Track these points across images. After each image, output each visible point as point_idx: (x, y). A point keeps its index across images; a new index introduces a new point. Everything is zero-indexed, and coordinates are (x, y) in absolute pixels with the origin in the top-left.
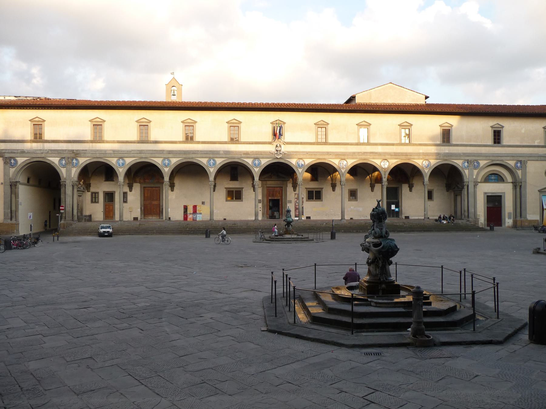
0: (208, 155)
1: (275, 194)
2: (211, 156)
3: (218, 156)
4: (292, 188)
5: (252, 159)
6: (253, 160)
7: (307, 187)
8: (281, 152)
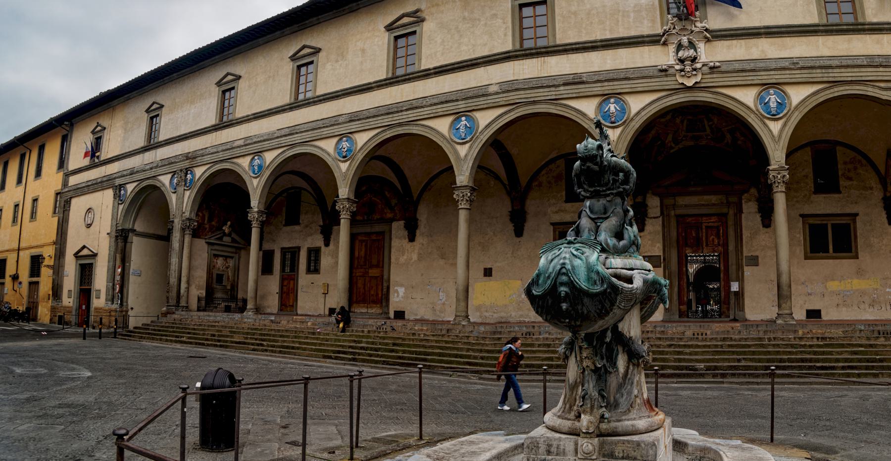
0: (450, 107)
1: (704, 239)
2: (462, 105)
3: (481, 102)
4: (758, 218)
5: (596, 102)
6: (600, 104)
8: (698, 66)
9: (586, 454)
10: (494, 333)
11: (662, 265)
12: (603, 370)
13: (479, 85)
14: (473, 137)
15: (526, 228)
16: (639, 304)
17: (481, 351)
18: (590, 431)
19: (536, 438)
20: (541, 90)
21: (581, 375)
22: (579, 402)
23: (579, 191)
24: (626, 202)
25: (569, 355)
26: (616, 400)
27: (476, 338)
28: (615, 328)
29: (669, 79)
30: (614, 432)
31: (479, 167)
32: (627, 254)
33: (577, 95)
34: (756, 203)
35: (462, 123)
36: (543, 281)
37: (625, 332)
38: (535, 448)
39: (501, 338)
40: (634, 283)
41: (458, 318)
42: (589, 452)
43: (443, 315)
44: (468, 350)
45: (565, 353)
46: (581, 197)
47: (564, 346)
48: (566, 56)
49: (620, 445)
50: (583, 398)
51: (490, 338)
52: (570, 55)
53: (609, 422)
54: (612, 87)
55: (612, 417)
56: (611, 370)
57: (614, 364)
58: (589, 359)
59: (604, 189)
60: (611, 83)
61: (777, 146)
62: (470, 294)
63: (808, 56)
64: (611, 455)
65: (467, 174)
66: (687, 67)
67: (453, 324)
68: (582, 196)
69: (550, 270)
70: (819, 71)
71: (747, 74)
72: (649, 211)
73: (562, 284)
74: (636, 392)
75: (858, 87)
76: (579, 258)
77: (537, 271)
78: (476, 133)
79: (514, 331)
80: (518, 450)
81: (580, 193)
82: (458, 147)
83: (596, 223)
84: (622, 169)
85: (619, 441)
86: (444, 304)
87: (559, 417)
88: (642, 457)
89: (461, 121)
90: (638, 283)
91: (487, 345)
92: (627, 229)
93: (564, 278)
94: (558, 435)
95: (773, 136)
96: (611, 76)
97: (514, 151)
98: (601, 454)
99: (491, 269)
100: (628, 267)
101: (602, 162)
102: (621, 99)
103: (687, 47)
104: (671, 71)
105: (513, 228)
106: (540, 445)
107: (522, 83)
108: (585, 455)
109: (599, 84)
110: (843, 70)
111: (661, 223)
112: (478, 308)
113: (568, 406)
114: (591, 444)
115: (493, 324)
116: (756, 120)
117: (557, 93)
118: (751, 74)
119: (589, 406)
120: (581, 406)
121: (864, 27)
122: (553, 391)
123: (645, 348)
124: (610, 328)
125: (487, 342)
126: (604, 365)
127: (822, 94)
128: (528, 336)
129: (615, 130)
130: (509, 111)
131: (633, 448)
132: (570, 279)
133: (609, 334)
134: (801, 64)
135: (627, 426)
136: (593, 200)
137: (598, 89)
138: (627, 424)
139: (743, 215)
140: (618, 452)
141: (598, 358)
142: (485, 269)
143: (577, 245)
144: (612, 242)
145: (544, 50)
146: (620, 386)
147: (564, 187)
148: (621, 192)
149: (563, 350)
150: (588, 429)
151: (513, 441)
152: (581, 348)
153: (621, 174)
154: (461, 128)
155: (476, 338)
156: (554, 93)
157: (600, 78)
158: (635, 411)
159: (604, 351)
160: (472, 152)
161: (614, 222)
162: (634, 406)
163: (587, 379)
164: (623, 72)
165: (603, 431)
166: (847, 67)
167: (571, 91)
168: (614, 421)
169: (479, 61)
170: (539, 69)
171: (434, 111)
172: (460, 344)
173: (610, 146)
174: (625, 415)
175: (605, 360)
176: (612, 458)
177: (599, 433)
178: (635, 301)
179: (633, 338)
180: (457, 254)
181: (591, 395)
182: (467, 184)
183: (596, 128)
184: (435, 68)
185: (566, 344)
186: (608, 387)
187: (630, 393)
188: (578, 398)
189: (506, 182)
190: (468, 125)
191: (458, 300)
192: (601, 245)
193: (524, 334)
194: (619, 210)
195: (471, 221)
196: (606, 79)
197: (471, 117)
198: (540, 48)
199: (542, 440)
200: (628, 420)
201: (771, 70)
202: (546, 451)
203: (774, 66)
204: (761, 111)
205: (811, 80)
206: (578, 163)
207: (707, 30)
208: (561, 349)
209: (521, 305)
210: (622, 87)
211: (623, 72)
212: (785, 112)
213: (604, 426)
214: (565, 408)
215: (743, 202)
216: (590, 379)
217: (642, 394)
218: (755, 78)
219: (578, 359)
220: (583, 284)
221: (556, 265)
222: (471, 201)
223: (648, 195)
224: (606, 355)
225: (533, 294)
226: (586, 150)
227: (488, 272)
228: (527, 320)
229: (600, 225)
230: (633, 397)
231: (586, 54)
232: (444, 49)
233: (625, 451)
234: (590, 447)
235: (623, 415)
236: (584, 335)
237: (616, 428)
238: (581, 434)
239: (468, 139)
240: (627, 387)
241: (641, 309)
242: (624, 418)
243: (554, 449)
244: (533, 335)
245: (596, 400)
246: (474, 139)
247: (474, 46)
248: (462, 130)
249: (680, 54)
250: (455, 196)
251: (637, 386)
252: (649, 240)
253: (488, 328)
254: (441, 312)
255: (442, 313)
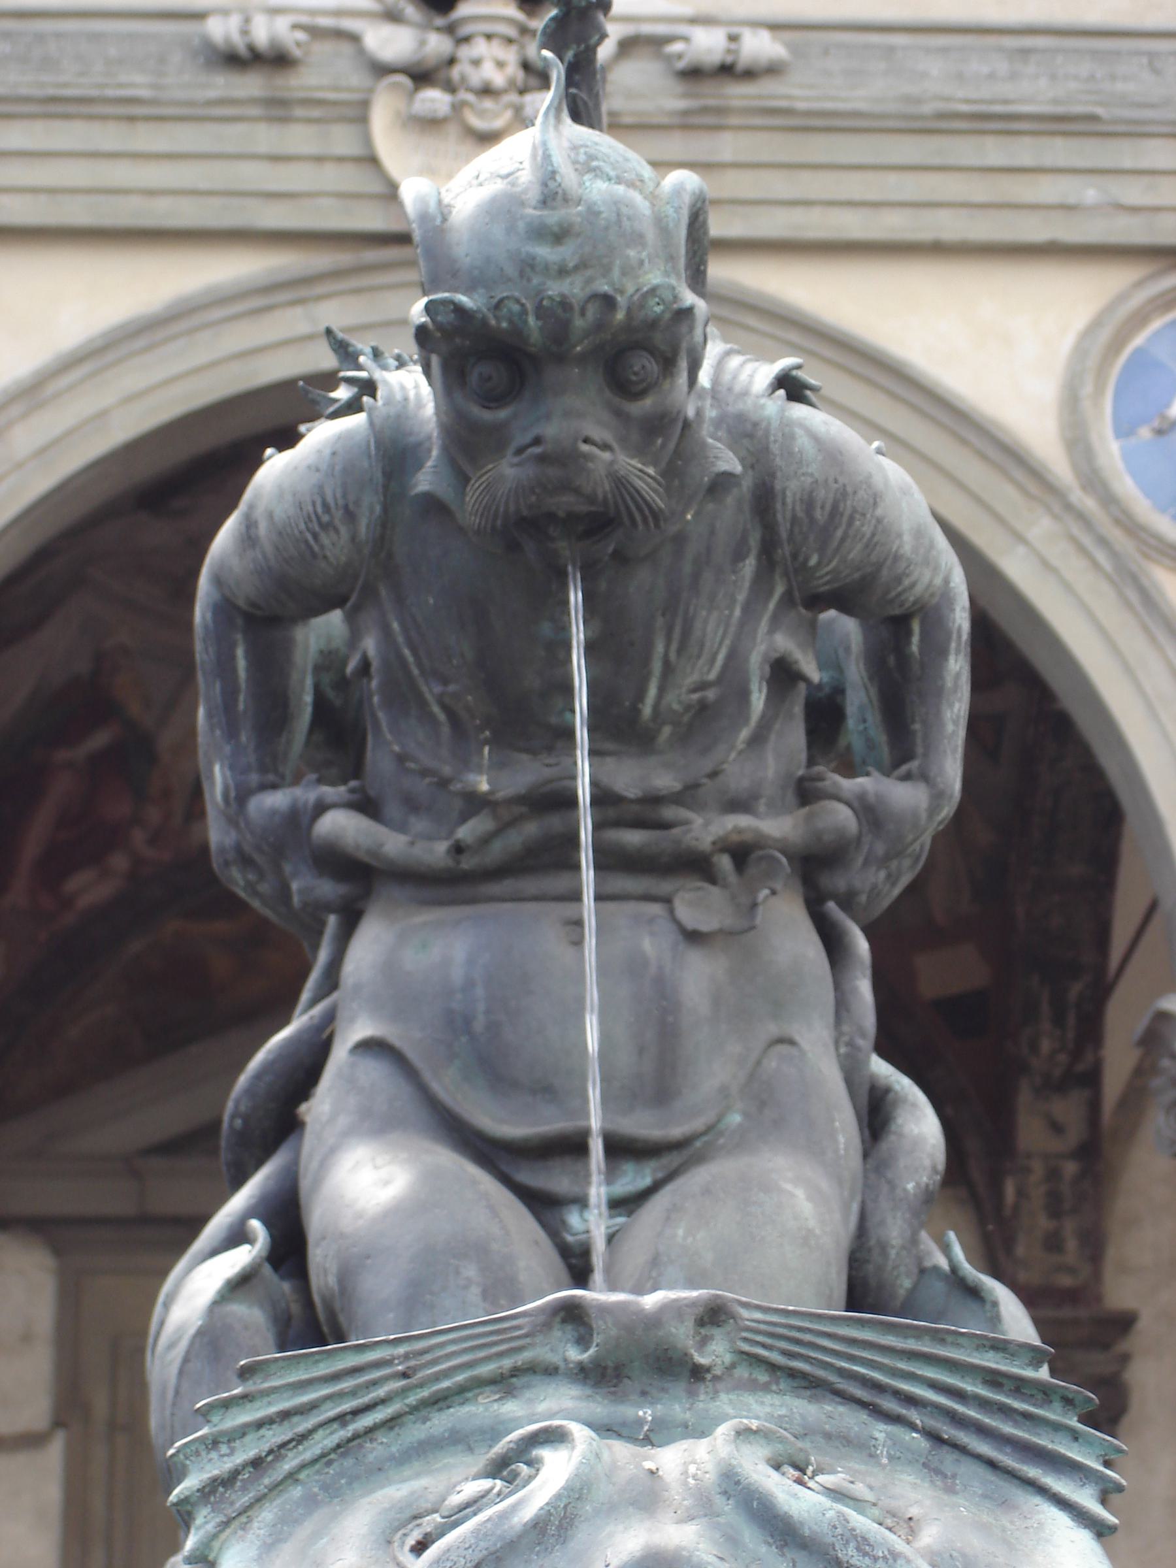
66: (480, 48)
71: (1024, 151)
116: (1074, 568)
118: (1059, 151)
204: (1127, 486)
218: (1090, 193)
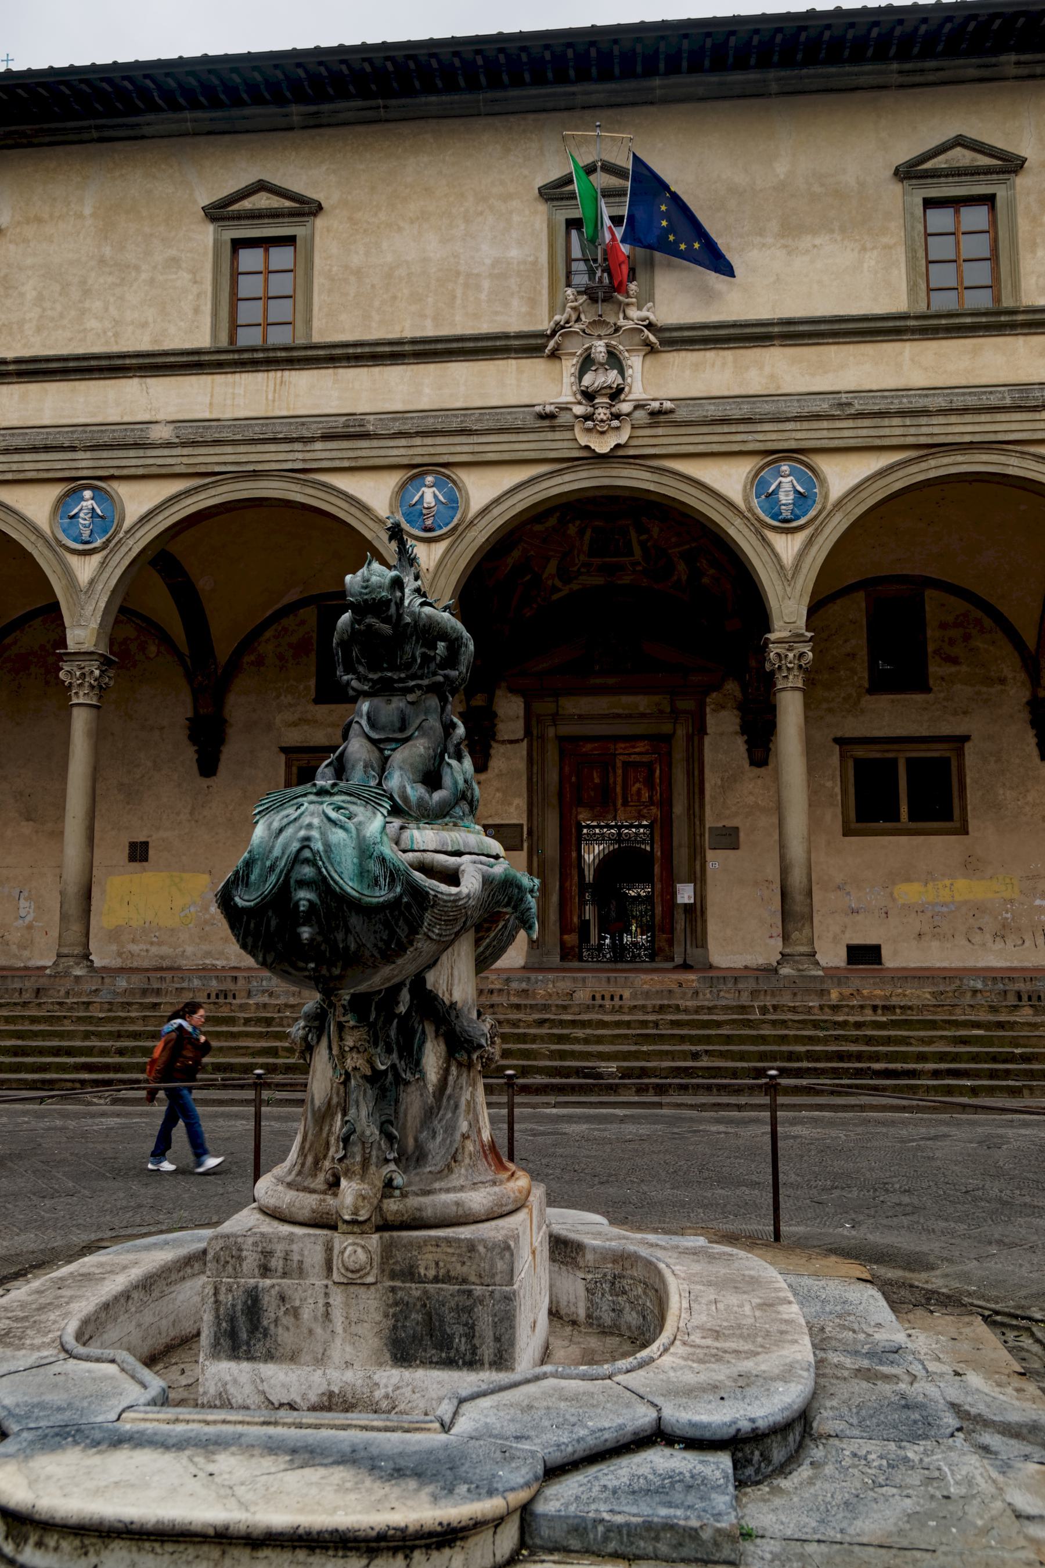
1: (619, 789)
2: (84, 463)
3: (131, 459)
4: (740, 745)
6: (403, 487)
7: (848, 734)
8: (625, 407)
9: (352, 1272)
10: (144, 992)
11: (525, 845)
12: (390, 1076)
13: (126, 419)
14: (109, 541)
15: (224, 757)
16: (471, 933)
17: (119, 1035)
18: (361, 1219)
19: (237, 1236)
20: (272, 447)
21: (342, 1088)
22: (336, 1151)
23: (345, 678)
24: (449, 707)
25: (314, 1043)
26: (419, 1146)
27: (106, 1006)
28: (418, 983)
29: (558, 435)
30: (414, 1219)
31: (122, 610)
32: (447, 819)
33: (353, 464)
34: (736, 712)
35: (84, 504)
36: (260, 876)
37: (442, 991)
38: (232, 1261)
39: (159, 1004)
40: (463, 881)
41: (63, 960)
42: (357, 1266)
43: (26, 953)
44: (87, 1035)
45: (305, 1038)
46: (351, 693)
47: (302, 1023)
48: (331, 371)
49: (430, 1248)
50: (346, 1140)
51: (141, 1004)
52: (341, 371)
53: (404, 1195)
54: (432, 450)
55: (410, 1184)
56: (408, 1076)
57: (416, 1064)
58: (359, 1052)
59: (403, 675)
60: (429, 441)
61: (789, 589)
62: (94, 902)
63: (875, 388)
64: (410, 1274)
65: (94, 624)
66: (600, 410)
67: (50, 976)
68: (354, 689)
69: (277, 852)
70: (896, 421)
72: (501, 726)
73: (302, 884)
74: (464, 1126)
75: (985, 458)
76: (342, 827)
77: (246, 854)
78: (116, 532)
79: (189, 989)
80: (192, 1267)
81: (348, 682)
82: (74, 561)
83: (381, 751)
84: (443, 634)
85: (426, 1241)
86: (30, 927)
87: (290, 1185)
88: (480, 1277)
89: (83, 499)
90: (470, 884)
91: (132, 1020)
92: (449, 764)
93: (307, 871)
94: (286, 1229)
95: (782, 567)
96: (430, 424)
97: (204, 584)
98: (387, 1273)
99: (145, 845)
100: (450, 849)
101: (400, 616)
102: (448, 477)
103: (602, 364)
104: (564, 418)
105: (196, 756)
106: (244, 1253)
107: (229, 427)
108: (350, 1275)
109: (403, 442)
110: (953, 419)
111: (525, 753)
112: (115, 935)
113: (310, 1160)
114: (363, 1247)
115: (147, 970)
116: (746, 531)
117: (308, 456)
118: (742, 428)
119: (358, 1158)
120: (341, 1160)
121: (1015, 318)
122: (276, 1125)
123: (486, 1027)
124: (408, 982)
125: (133, 1014)
126: (393, 1066)
127: (900, 474)
128: (221, 1000)
129: (433, 545)
130: (196, 490)
131: (460, 1255)
132: (321, 872)
133: (405, 996)
134: (857, 407)
135: (445, 1205)
136: (377, 701)
137: (399, 451)
138: (444, 1200)
139: (707, 740)
140: (426, 1266)
141: (379, 1050)
142: (133, 846)
143: (337, 799)
144: (415, 792)
145: (283, 354)
146: (430, 1114)
147: (313, 669)
148: (439, 683)
149: (301, 1032)
150: (355, 1213)
151: (181, 1245)
152: (341, 1027)
153: (441, 645)
154: (82, 515)
155: (106, 1006)
156: (300, 456)
157: (406, 427)
158: (463, 1171)
159: (393, 1033)
160: (106, 575)
161: (422, 750)
162: (459, 1158)
163: (354, 1096)
164: (456, 416)
165: (390, 1218)
166: (965, 411)
167: (339, 454)
168: (417, 1195)
169: (128, 361)
170: (270, 397)
171: (14, 467)
172: (66, 1022)
173: (419, 582)
174: (441, 1179)
175: (395, 1055)
176: (412, 1281)
177: (381, 1223)
178: (465, 923)
179: (459, 1005)
180: (64, 808)
181: (363, 1132)
182: (92, 649)
183: (391, 539)
184: (18, 361)
185: (308, 1017)
186: (401, 1115)
187: (451, 1128)
188: (332, 1140)
189: (184, 648)
190: (99, 511)
191: (64, 917)
192: (391, 798)
193: (213, 995)
194: (434, 723)
195: (99, 736)
196: (420, 429)
197: (107, 492)
198: (274, 349)
199: (250, 1241)
200: (448, 1191)
201: (788, 420)
202: (260, 1266)
203: (794, 410)
204: (759, 511)
205: (878, 442)
206: (347, 616)
207: (650, 326)
208: (297, 1030)
209: (207, 928)
210: (453, 449)
211: (456, 416)
212: (812, 513)
213: (392, 1206)
214: (303, 1165)
215: (708, 710)
216: (361, 1098)
217: (479, 1132)
218: (750, 437)
219: (335, 1052)
220: (350, 885)
221: (290, 841)
222: (101, 690)
223: (499, 693)
224: (398, 1043)
225: (236, 904)
226: (366, 587)
227: (139, 852)
228: (219, 963)
229: (389, 756)
230: (458, 1137)
231: (376, 370)
232: (41, 317)
233: (441, 1264)
234: (362, 1256)
235: (436, 1180)
236: (348, 997)
237: (419, 1210)
238: (340, 1224)
239: (98, 543)
240: (444, 1115)
241: (477, 942)
242: (437, 1185)
243: (276, 1263)
244: (234, 997)
245: (375, 1146)
246: (111, 545)
247: (117, 322)
248: (84, 520)
249: (587, 380)
250: (62, 675)
251: (468, 1112)
252: (498, 790)
253: (137, 981)
254: (22, 947)
255: (25, 948)
